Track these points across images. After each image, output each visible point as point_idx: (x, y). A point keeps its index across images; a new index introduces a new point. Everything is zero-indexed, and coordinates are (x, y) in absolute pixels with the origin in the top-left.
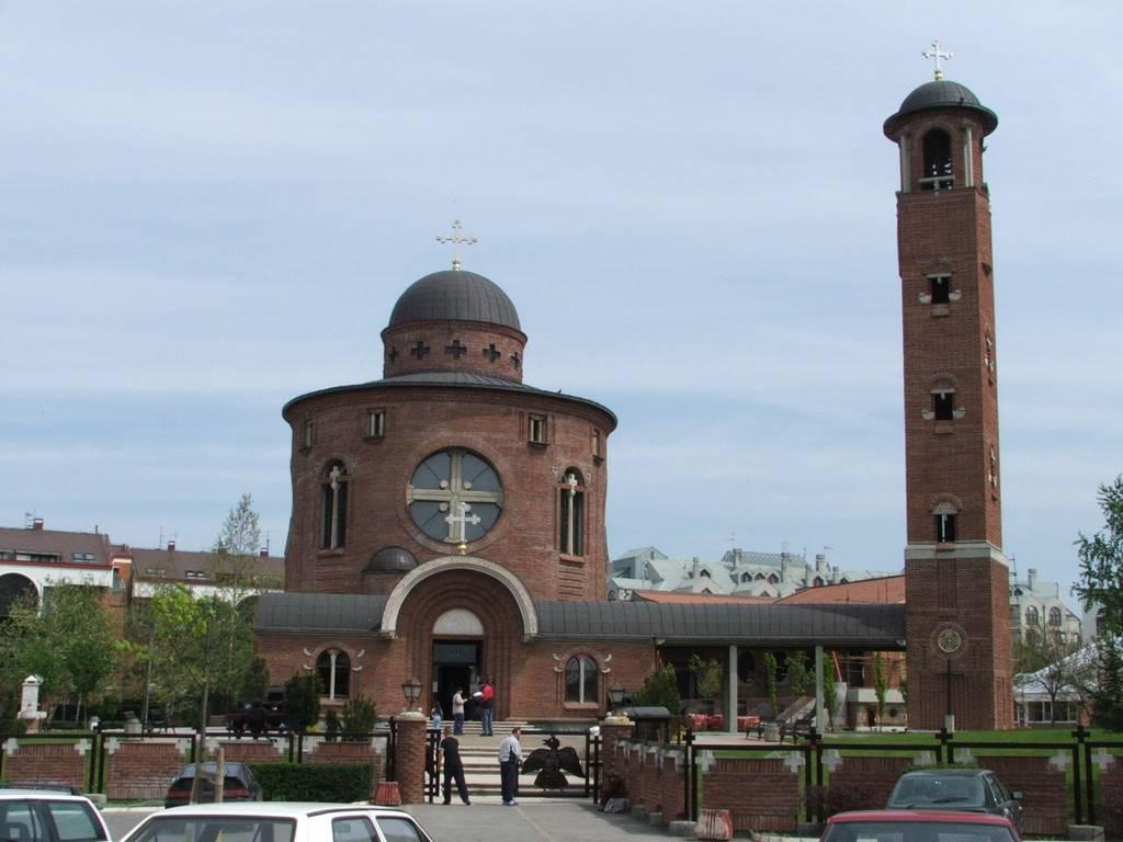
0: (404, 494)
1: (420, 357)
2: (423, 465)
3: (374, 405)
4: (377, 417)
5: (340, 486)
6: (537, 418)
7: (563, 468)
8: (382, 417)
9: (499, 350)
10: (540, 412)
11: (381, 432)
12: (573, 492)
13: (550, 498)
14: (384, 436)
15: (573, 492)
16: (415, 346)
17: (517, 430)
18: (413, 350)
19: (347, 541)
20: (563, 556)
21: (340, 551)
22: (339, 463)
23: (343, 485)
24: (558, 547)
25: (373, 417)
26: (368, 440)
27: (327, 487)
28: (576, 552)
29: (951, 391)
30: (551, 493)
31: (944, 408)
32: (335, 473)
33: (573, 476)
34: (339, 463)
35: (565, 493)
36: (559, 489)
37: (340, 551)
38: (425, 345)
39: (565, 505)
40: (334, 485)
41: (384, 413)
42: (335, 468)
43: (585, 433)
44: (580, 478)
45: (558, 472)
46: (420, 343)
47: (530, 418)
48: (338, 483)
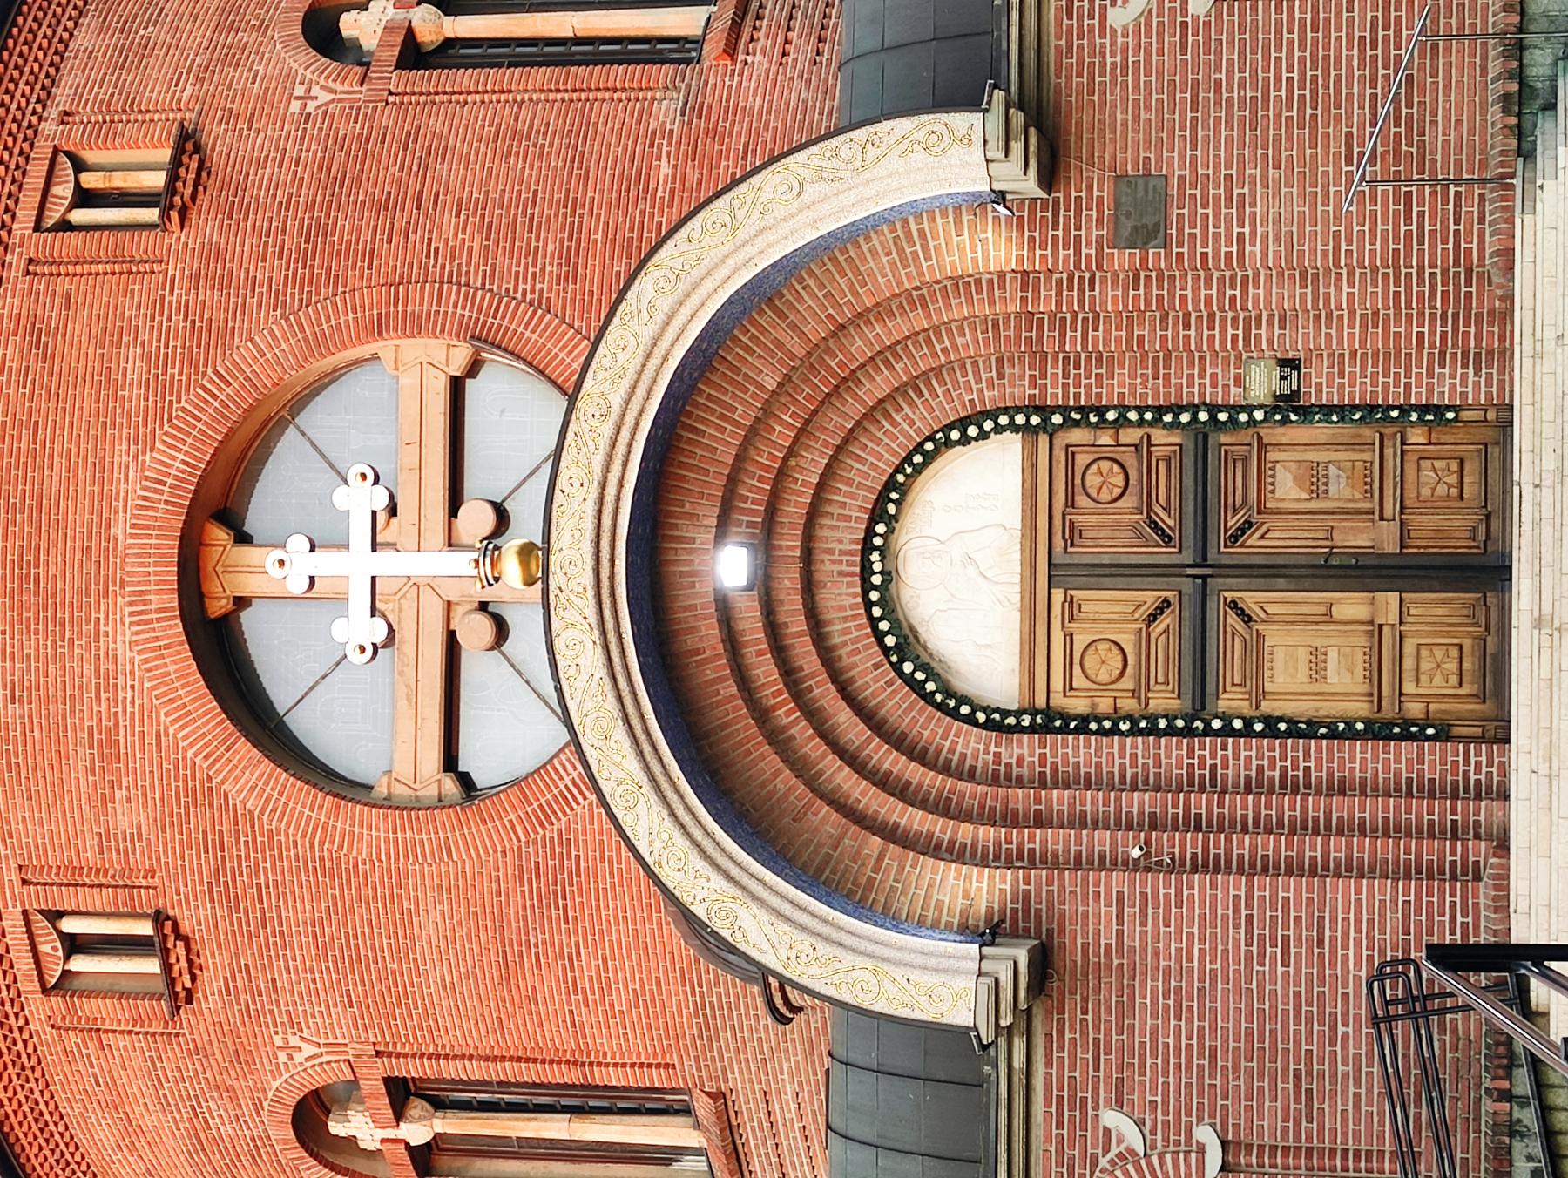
4: (75, 945)
5: (417, 1107)
6: (64, 190)
7: (302, 61)
8: (70, 925)
11: (145, 928)
14: (159, 918)
17: (105, 290)
19: (658, 1079)
21: (703, 1106)
25: (79, 963)
37: (703, 1106)
39: (449, 53)
40: (417, 1132)
47: (65, 226)
48: (399, 1115)
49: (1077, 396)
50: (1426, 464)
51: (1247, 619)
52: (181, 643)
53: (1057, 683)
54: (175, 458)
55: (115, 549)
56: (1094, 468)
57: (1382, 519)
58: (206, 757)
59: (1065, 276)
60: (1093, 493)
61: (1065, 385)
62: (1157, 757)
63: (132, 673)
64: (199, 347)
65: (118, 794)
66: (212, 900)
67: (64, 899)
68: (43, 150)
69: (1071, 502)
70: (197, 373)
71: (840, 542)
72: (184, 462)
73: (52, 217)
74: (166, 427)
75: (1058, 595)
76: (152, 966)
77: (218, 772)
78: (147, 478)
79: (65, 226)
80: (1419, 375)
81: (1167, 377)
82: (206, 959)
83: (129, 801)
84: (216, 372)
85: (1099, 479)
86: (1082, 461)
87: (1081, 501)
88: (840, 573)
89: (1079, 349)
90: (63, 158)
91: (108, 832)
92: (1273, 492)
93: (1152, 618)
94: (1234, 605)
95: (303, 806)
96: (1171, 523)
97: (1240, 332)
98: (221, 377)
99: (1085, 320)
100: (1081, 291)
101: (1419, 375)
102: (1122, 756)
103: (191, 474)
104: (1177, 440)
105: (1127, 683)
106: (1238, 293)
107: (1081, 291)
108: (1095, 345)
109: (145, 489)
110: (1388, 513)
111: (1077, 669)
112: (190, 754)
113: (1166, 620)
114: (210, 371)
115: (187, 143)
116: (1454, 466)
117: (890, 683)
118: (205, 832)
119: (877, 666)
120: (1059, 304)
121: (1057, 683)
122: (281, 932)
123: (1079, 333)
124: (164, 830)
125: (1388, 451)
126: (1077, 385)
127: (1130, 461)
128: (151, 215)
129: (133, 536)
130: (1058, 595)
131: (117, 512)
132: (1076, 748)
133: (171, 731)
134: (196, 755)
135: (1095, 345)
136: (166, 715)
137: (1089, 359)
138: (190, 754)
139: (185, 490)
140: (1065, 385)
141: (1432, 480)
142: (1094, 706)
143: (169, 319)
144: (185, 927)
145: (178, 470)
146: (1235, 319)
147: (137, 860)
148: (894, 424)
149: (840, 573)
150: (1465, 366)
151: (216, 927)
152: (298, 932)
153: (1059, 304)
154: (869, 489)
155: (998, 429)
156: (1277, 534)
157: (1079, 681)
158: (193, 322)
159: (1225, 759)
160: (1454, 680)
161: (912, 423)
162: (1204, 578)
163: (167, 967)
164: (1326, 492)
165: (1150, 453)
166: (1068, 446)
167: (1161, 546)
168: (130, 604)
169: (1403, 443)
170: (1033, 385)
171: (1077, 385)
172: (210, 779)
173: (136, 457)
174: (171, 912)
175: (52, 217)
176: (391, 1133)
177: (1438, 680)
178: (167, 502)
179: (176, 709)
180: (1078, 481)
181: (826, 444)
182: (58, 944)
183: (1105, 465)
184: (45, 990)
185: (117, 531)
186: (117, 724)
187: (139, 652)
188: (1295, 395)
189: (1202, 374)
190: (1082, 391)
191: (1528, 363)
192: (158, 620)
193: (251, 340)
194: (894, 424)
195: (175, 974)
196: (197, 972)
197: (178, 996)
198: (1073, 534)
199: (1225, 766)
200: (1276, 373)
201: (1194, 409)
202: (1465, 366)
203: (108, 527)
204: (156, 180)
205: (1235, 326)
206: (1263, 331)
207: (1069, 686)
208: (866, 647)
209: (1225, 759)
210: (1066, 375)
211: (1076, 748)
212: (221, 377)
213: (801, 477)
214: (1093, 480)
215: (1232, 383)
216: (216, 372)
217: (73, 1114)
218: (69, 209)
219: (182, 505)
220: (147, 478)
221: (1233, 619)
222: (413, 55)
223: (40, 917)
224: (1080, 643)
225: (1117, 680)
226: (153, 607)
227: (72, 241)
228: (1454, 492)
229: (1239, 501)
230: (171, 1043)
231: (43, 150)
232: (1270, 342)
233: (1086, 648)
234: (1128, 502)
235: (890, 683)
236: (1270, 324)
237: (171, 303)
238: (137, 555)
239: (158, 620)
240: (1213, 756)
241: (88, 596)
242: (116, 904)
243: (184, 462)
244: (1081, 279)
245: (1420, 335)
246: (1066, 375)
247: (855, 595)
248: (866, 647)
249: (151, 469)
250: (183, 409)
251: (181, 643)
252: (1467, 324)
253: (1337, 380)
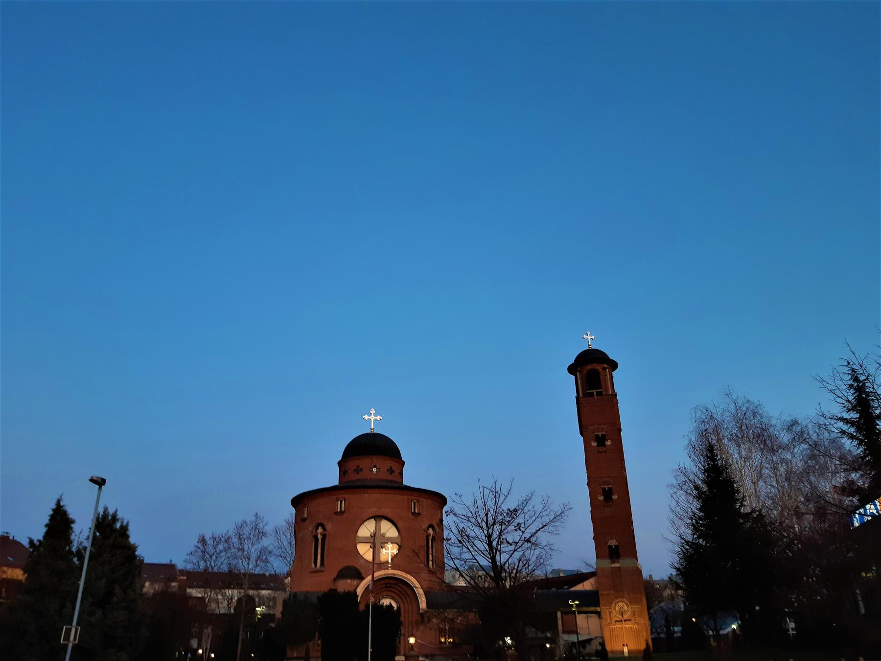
1: (358, 473)
3: (340, 496)
4: (341, 502)
5: (322, 536)
6: (415, 501)
8: (343, 502)
9: (394, 469)
14: (344, 511)
16: (355, 468)
18: (355, 470)
21: (322, 569)
22: (323, 526)
23: (324, 537)
25: (339, 502)
26: (336, 513)
29: (611, 486)
31: (608, 494)
32: (320, 530)
34: (323, 526)
37: (322, 569)
38: (361, 467)
40: (319, 536)
41: (345, 500)
42: (320, 528)
45: (424, 526)
46: (358, 467)
48: (321, 535)
79: (412, 501)
115: (419, 514)
128: (413, 511)
176: (319, 533)
204: (416, 511)
222: (428, 536)
227: (410, 501)
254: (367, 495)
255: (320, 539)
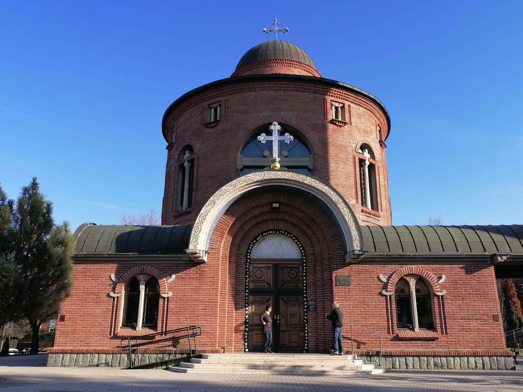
0: (235, 160)
2: (251, 144)
4: (216, 110)
6: (337, 105)
8: (218, 108)
10: (340, 100)
11: (218, 119)
12: (367, 163)
13: (351, 163)
15: (367, 163)
20: (364, 208)
22: (189, 148)
23: (192, 161)
24: (360, 201)
25: (213, 110)
26: (207, 125)
27: (182, 167)
28: (372, 208)
30: (352, 160)
32: (187, 154)
33: (367, 150)
35: (362, 162)
36: (357, 158)
41: (220, 105)
42: (187, 152)
43: (372, 122)
44: (371, 152)
47: (332, 105)
49: (308, 269)
50: (297, 335)
51: (267, 301)
52: (264, 123)
53: (255, 265)
54: (294, 122)
55: (279, 112)
56: (295, 272)
57: (286, 327)
58: (245, 128)
59: (331, 266)
60: (290, 272)
61: (310, 267)
62: (241, 284)
63: (259, 116)
64: (312, 125)
65: (239, 114)
66: (222, 130)
67: (223, 106)
68: (344, 102)
69: (288, 268)
70: (308, 125)
71: (280, 225)
72: (293, 123)
73: (333, 103)
74: (299, 120)
75: (271, 265)
76: (212, 120)
77: (243, 130)
78: (290, 117)
79: (332, 105)
80: (314, 334)
81: (312, 286)
82: (213, 130)
83: (238, 116)
84: (308, 128)
85: (292, 273)
86: (296, 270)
87: (289, 270)
88: (275, 225)
89: (317, 269)
90: (342, 105)
91: (233, 113)
92: (291, 306)
93: (267, 283)
94: (270, 299)
95: (237, 143)
96: (285, 287)
97: (321, 300)
98: (308, 129)
99: (323, 270)
100: (328, 269)
101: (314, 334)
102: (242, 278)
103: (291, 124)
104: (300, 288)
105: (255, 278)
106: (329, 299)
107: (328, 269)
108: (318, 272)
109: (289, 117)
110: (288, 328)
111: (258, 269)
112: (246, 125)
113: (266, 284)
114: (308, 127)
116: (296, 341)
117: (255, 234)
118: (233, 128)
119: (258, 232)
120: (325, 265)
121: (255, 265)
122: (217, 141)
123: (320, 269)
124: (233, 122)
125: (299, 328)
126: (310, 269)
127: (296, 279)
129: (281, 115)
130: (271, 265)
131: (285, 113)
132: (243, 269)
133: (250, 122)
134: (246, 126)
135: (318, 272)
136: (252, 121)
137: (315, 271)
138: (246, 125)
139: (289, 123)
140: (310, 267)
141: (294, 338)
142: (251, 272)
143: (317, 121)
144: (218, 126)
145: (292, 122)
146: (323, 299)
147: (229, 118)
148: (302, 235)
149: (275, 225)
150: (316, 343)
151: (218, 130)
152: (217, 143)
153: (325, 265)
154: (290, 231)
155: (302, 253)
156: (283, 307)
157: (256, 269)
158: (316, 125)
159: (241, 297)
160: (256, 341)
161: (302, 238)
162: (275, 293)
163: (212, 123)
164: (291, 316)
165: (298, 283)
166: (299, 267)
167: (281, 284)
168: (270, 115)
169: (300, 331)
170: (310, 260)
171: (310, 269)
172: (242, 128)
173: (294, 115)
174: (220, 123)
175: (333, 103)
177: (256, 338)
178: (287, 120)
179: (253, 123)
180: (292, 269)
181: (298, 223)
182: (216, 106)
183: (295, 274)
184: (209, 105)
185: (282, 113)
186: (250, 113)
187: (262, 117)
188: (309, 310)
189: (313, 292)
190: (309, 270)
191: (317, 358)
192: (267, 120)
193: (314, 134)
194: (302, 235)
195: (211, 124)
196: (211, 128)
197: (207, 125)
198: (283, 268)
199: (240, 297)
200: (313, 307)
201: (306, 290)
202: (316, 343)
203: (282, 111)
205: (322, 299)
206: (321, 304)
207: (254, 267)
208: (261, 230)
209: (241, 297)
210: (312, 267)
211: (243, 269)
212: (308, 129)
213: (292, 218)
214: (292, 272)
215: (311, 298)
216: (308, 128)
217: (189, 111)
218: (334, 105)
219: (286, 123)
220: (290, 117)
221: (267, 298)
223: (220, 103)
224: (263, 270)
225: (256, 276)
226: (269, 119)
228: (292, 341)
229: (289, 299)
230: (200, 125)
231: (344, 102)
232: (319, 305)
233: (261, 271)
234: (289, 278)
235: (255, 234)
236: (323, 306)
237: (319, 121)
238: (278, 116)
239: (267, 120)
240: (241, 295)
241: (271, 108)
242: (222, 115)
243: (293, 123)
244: (330, 269)
245: (321, 335)
246: (312, 267)
247: (271, 228)
248: (261, 230)
249: (292, 118)
250: (302, 123)
251: (264, 123)
252: (324, 344)
253: (312, 318)
254: (254, 93)
255: (187, 168)
